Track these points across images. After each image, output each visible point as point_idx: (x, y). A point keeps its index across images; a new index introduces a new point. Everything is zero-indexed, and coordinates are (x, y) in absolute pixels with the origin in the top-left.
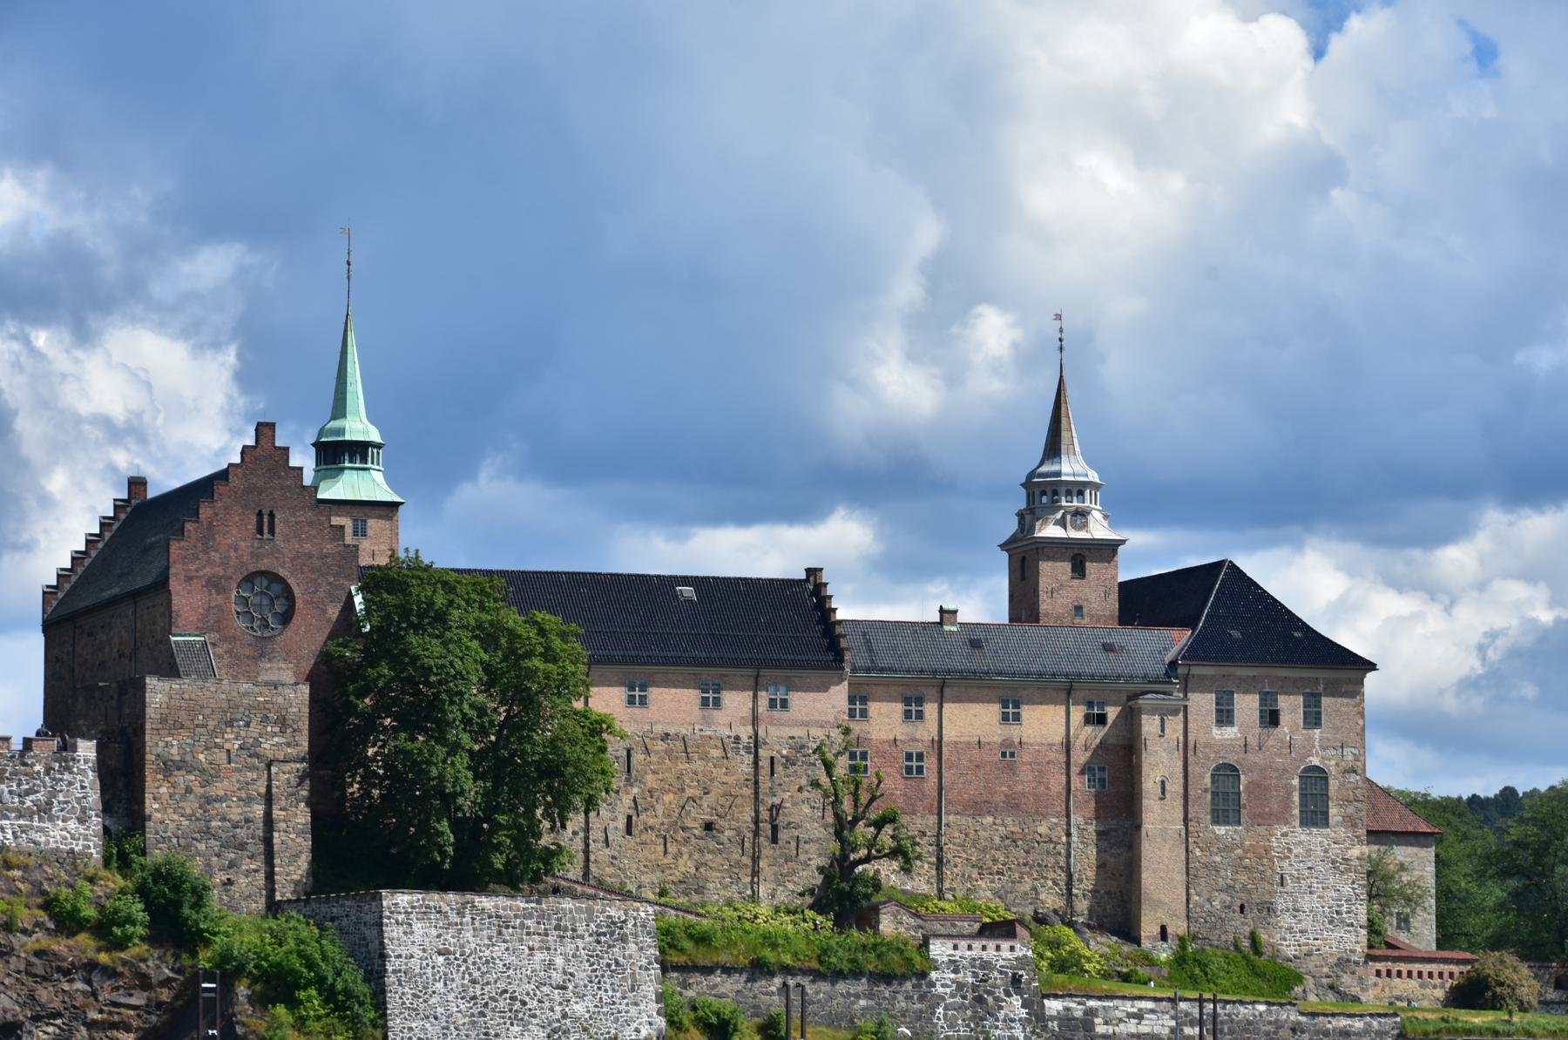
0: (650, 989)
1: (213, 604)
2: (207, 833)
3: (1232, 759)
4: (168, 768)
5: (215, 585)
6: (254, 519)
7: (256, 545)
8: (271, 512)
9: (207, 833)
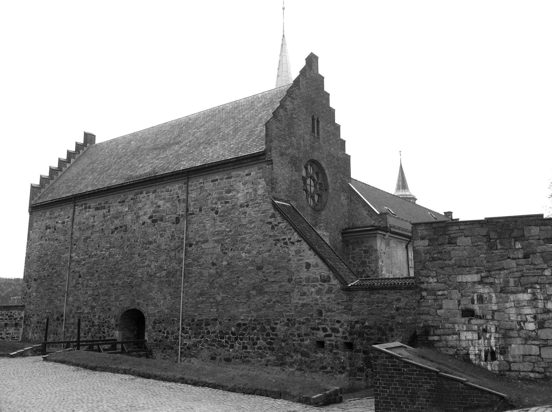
1: (294, 178)
5: (294, 163)
6: (311, 119)
7: (312, 140)
8: (318, 118)
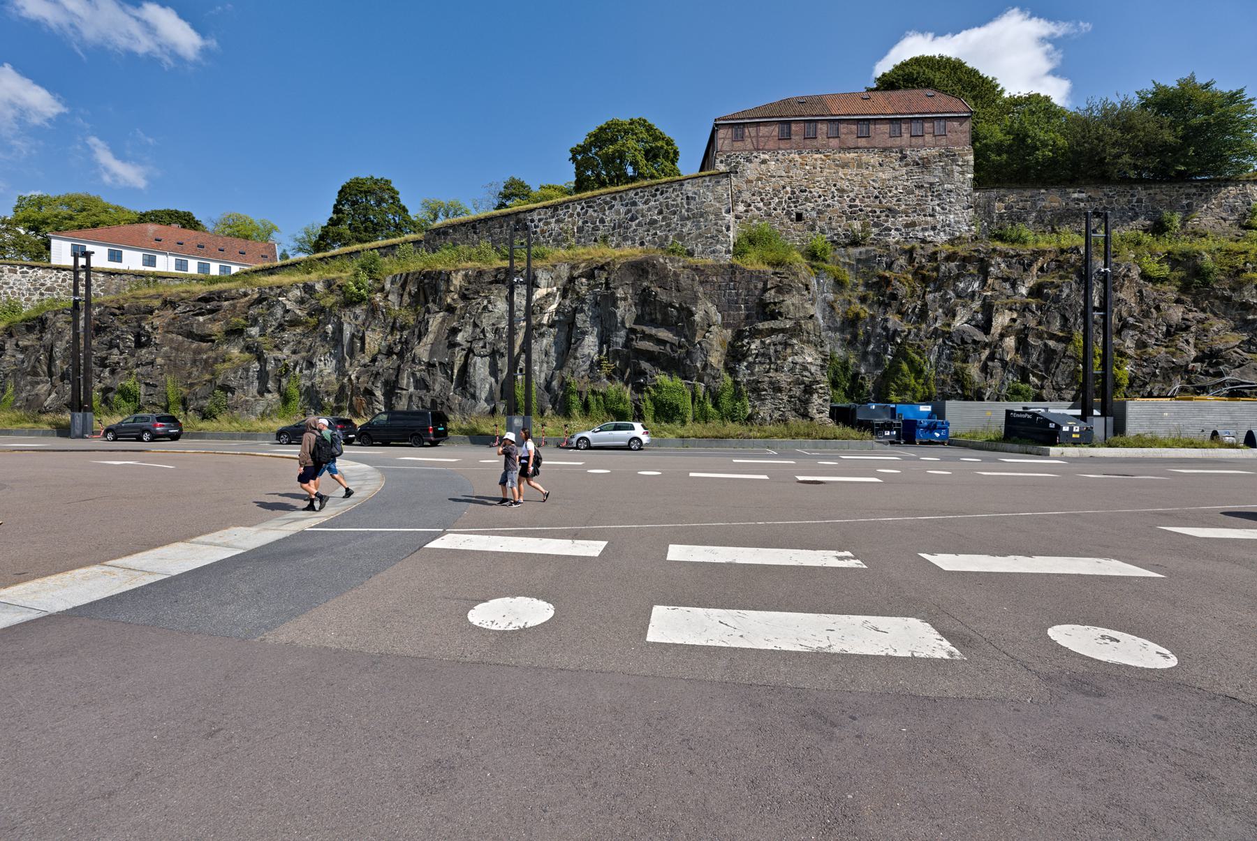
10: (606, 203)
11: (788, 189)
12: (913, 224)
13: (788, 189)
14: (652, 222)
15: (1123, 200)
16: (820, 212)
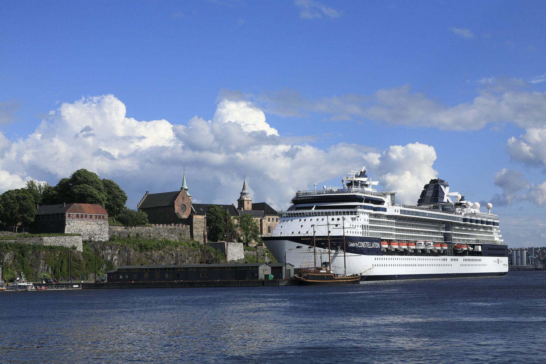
0: (243, 253)
2: (198, 235)
3: (270, 226)
4: (195, 228)
9: (198, 235)
10: (60, 238)
11: (78, 229)
12: (99, 237)
13: (78, 229)
14: (69, 243)
15: (131, 229)
16: (84, 234)
